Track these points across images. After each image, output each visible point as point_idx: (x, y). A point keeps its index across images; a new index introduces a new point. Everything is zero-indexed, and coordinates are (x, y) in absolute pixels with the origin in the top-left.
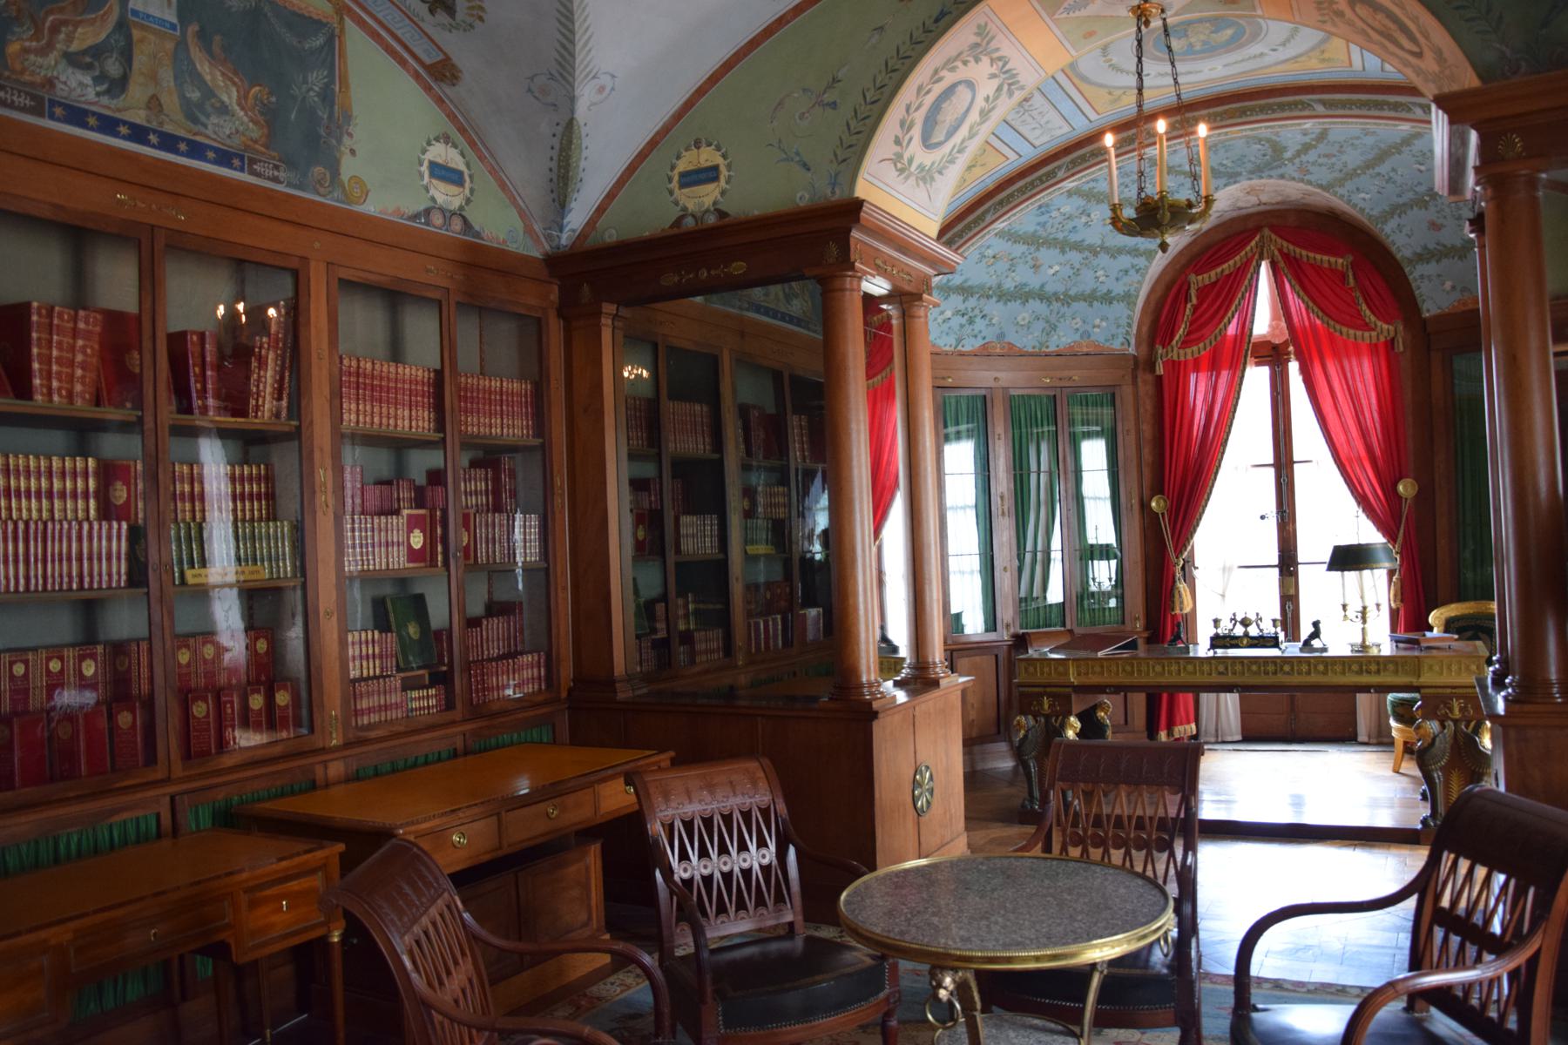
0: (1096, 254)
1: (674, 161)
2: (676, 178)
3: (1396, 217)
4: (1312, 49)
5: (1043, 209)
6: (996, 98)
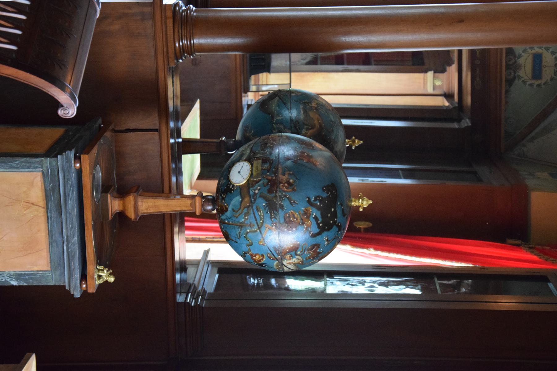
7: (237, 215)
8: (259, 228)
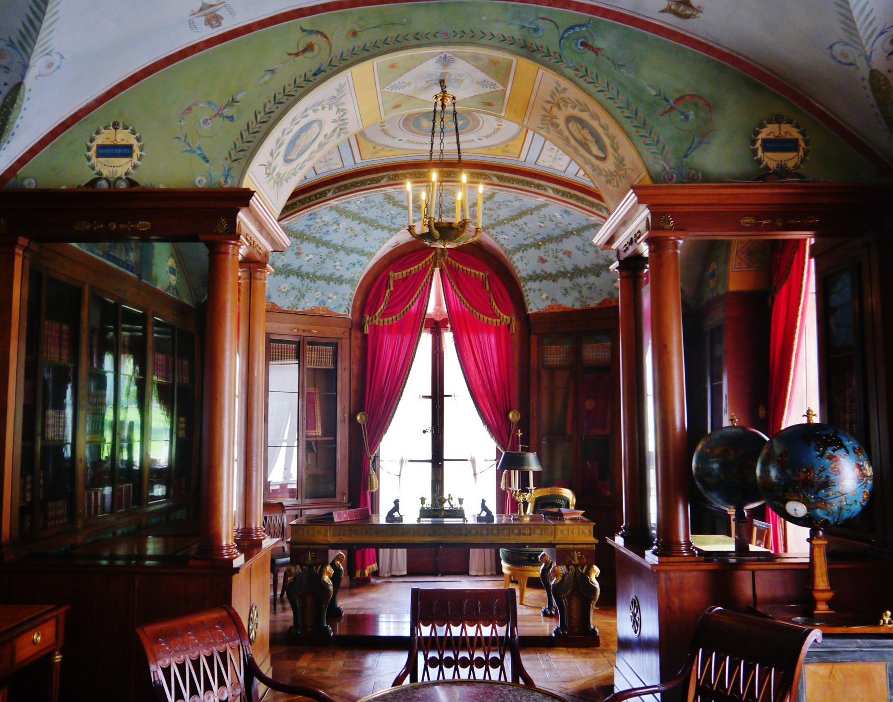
0: (337, 250)
1: (94, 135)
2: (94, 149)
3: (521, 251)
4: (502, 143)
5: (312, 216)
6: (331, 137)
7: (831, 512)
8: (843, 495)
